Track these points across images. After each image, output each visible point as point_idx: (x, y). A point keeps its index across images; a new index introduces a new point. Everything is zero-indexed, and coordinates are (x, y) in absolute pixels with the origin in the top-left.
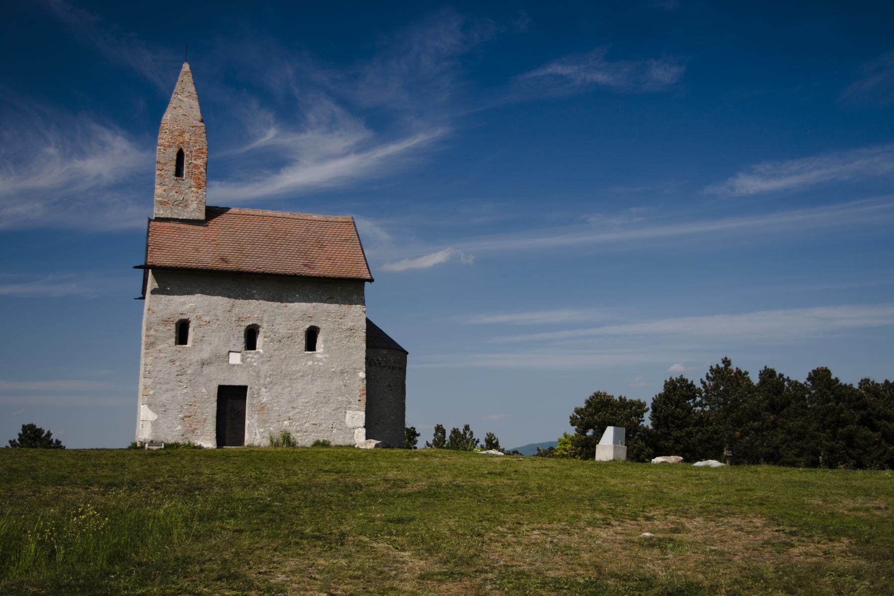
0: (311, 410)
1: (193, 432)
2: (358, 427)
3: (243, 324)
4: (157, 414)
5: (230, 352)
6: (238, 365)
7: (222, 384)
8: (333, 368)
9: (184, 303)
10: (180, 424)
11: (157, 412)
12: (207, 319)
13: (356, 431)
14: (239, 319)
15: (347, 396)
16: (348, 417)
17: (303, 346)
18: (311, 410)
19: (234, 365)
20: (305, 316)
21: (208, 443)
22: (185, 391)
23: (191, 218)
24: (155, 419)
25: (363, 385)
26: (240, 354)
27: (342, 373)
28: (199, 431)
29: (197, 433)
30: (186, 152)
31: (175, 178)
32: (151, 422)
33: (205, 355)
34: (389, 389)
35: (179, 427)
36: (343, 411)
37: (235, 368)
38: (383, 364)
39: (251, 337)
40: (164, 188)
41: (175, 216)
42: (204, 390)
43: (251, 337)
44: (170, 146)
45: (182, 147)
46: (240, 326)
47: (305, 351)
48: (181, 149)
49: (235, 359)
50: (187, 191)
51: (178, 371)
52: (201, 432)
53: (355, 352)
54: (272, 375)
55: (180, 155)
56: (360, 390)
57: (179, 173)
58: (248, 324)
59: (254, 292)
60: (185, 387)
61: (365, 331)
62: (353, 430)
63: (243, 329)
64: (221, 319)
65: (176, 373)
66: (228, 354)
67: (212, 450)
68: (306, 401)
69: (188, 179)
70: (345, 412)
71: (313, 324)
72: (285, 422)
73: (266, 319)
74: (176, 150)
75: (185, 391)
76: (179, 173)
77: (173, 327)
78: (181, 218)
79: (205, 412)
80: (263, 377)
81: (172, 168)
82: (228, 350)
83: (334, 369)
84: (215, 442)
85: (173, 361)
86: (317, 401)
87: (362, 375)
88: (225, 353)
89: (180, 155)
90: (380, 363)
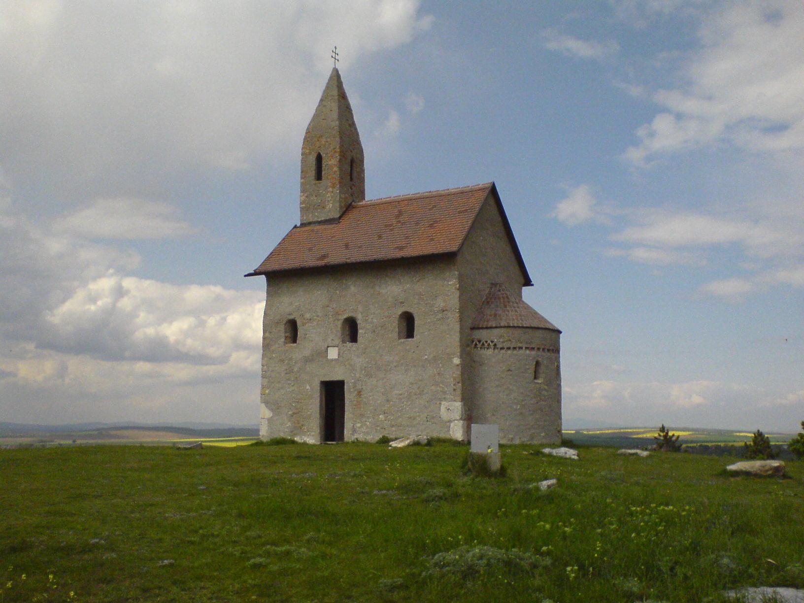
0: (405, 403)
1: (301, 428)
2: (454, 420)
3: (340, 317)
4: (273, 412)
5: (328, 347)
6: (335, 360)
7: (322, 380)
8: (426, 355)
9: (291, 304)
10: (289, 421)
11: (272, 410)
12: (308, 316)
13: (452, 425)
14: (337, 313)
15: (441, 385)
16: (443, 408)
18: (405, 403)
19: (332, 360)
21: (311, 437)
22: (293, 388)
23: (327, 218)
24: (270, 416)
25: (458, 373)
26: (337, 349)
27: (435, 359)
28: (305, 428)
29: (304, 429)
30: (324, 155)
31: (314, 182)
32: (269, 420)
33: (307, 353)
34: (510, 373)
35: (289, 424)
36: (438, 403)
38: (499, 346)
39: (351, 329)
40: (306, 195)
41: (316, 219)
42: (308, 387)
43: (351, 329)
44: (310, 153)
45: (320, 152)
46: (338, 320)
47: (399, 339)
49: (333, 354)
50: (324, 192)
51: (286, 370)
52: (307, 428)
54: (367, 367)
55: (319, 159)
56: (455, 379)
57: (319, 176)
58: (345, 317)
59: (350, 283)
60: (292, 384)
62: (448, 424)
63: (339, 324)
64: (320, 314)
65: (285, 372)
66: (327, 349)
67: (314, 445)
68: (401, 392)
69: (324, 182)
70: (440, 404)
72: (380, 416)
73: (360, 309)
74: (315, 155)
75: (293, 388)
76: (319, 176)
77: (282, 328)
78: (320, 220)
79: (310, 408)
81: (312, 173)
82: (326, 346)
83: (427, 357)
84: (319, 438)
85: (282, 361)
86: (411, 393)
87: (457, 361)
89: (319, 159)
90: (495, 345)
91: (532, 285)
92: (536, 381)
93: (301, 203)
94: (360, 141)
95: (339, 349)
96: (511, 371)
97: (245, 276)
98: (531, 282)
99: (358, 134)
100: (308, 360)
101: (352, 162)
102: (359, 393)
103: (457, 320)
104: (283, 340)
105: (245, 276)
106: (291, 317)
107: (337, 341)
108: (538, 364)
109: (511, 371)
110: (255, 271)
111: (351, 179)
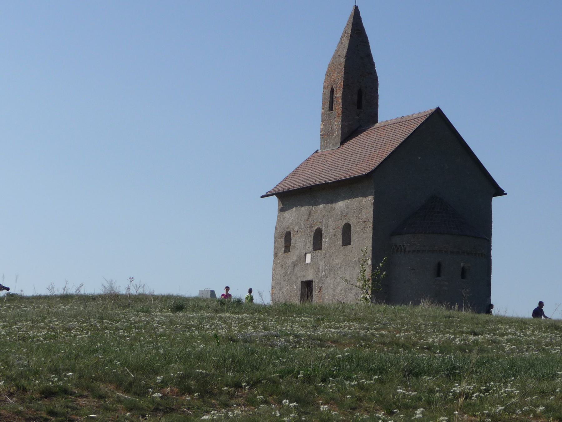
12: (296, 229)
17: (340, 242)
20: (344, 216)
26: (310, 254)
30: (335, 88)
33: (295, 258)
37: (308, 266)
38: (408, 249)
42: (295, 287)
48: (332, 86)
53: (367, 242)
55: (332, 91)
59: (320, 201)
61: (372, 221)
71: (346, 221)
73: (324, 222)
76: (331, 108)
80: (321, 271)
81: (327, 105)
82: (304, 253)
88: (303, 254)
90: (405, 249)
91: (506, 194)
92: (438, 278)
93: (321, 132)
94: (375, 71)
95: (311, 255)
96: (415, 270)
97: (263, 197)
98: (504, 191)
99: (373, 65)
100: (295, 265)
101: (360, 94)
102: (320, 290)
103: (371, 229)
104: (284, 249)
105: (262, 197)
106: (288, 230)
107: (311, 248)
108: (439, 265)
109: (415, 270)
110: (267, 193)
111: (359, 106)
